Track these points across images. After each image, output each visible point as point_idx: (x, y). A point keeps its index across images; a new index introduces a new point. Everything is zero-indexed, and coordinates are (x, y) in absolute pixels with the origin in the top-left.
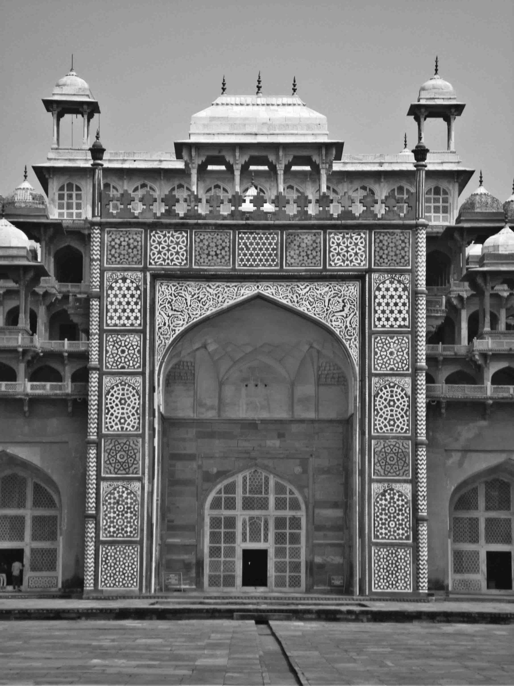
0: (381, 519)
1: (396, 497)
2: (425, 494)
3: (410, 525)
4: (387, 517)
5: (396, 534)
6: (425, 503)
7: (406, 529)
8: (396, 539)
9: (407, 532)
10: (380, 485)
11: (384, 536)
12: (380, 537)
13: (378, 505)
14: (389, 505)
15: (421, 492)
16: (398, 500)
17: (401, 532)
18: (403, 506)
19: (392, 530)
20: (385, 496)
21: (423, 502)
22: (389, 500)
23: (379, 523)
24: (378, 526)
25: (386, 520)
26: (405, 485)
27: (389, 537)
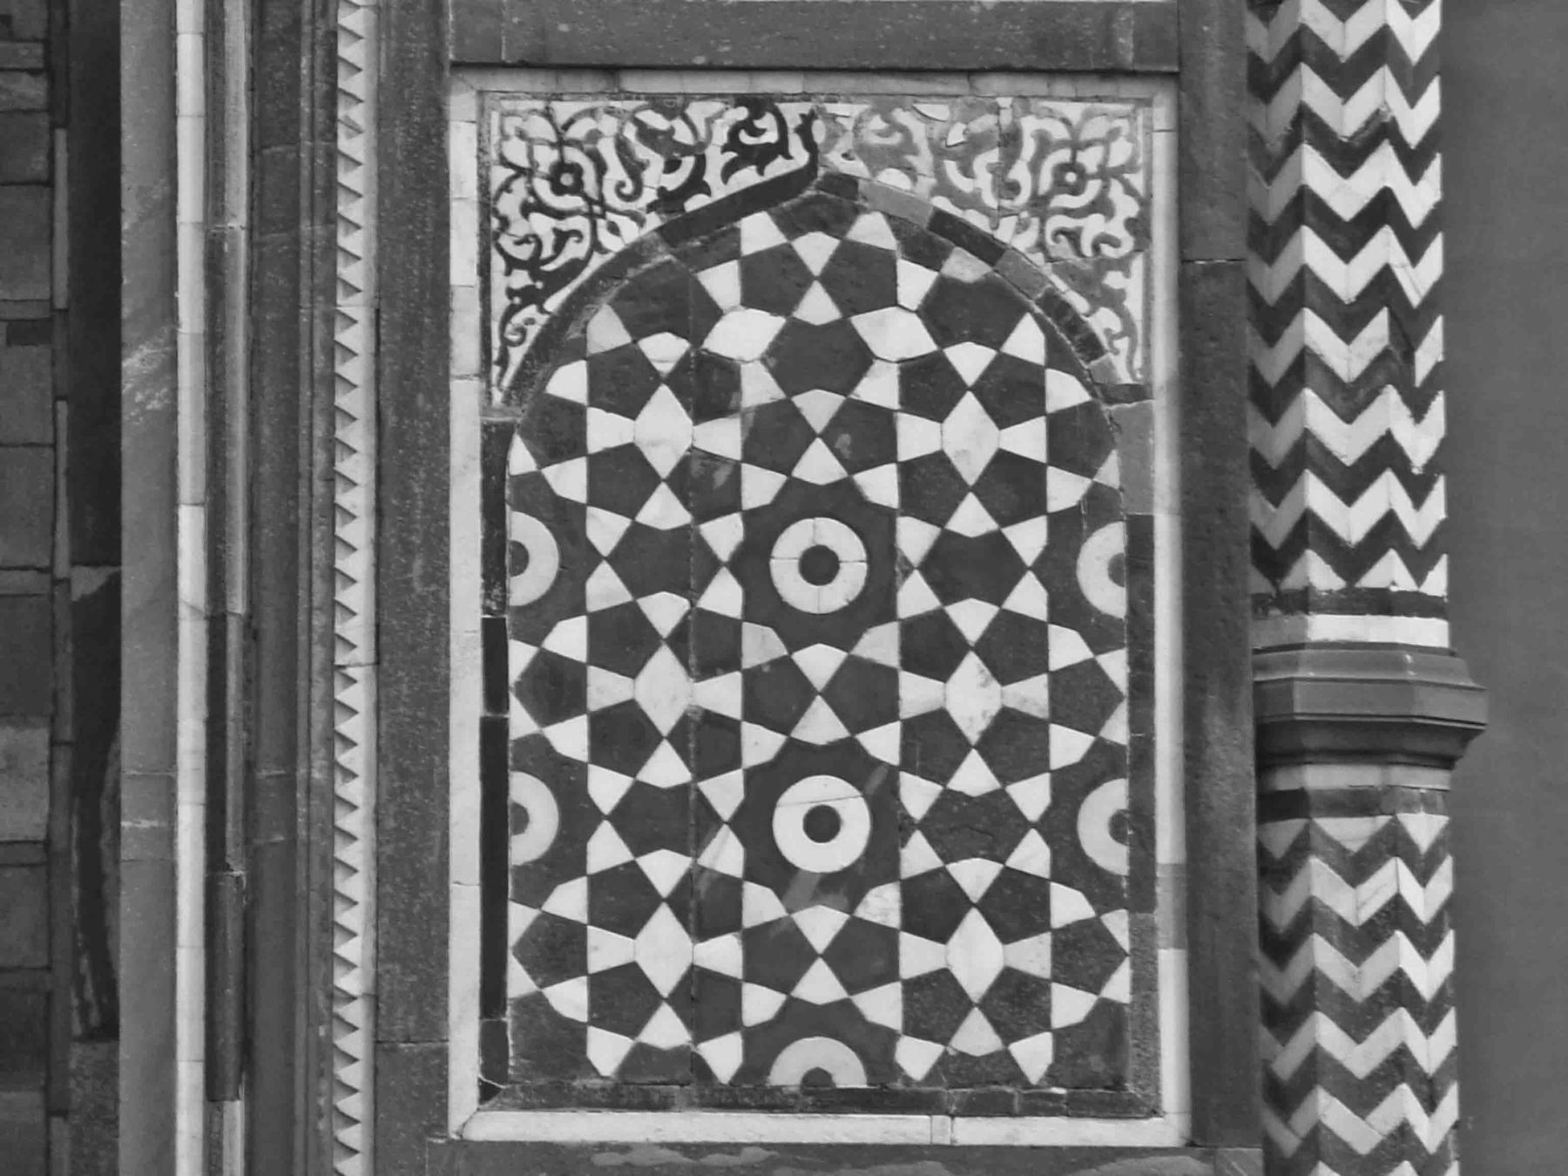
0: (624, 735)
1: (896, 334)
2: (1419, 278)
3: (1134, 826)
4: (723, 694)
5: (882, 1006)
6: (1421, 440)
7: (1068, 905)
8: (886, 1093)
9: (1082, 955)
10: (599, 120)
11: (666, 1030)
12: (607, 1051)
13: (570, 480)
14: (760, 487)
15: (1348, 238)
16: (929, 388)
17: (976, 955)
18: (1014, 486)
19: (821, 924)
20: (694, 316)
21: (1388, 413)
22: (758, 388)
23: (578, 817)
24: (565, 859)
25: (709, 741)
26: (1053, 115)
27: (763, 1044)
